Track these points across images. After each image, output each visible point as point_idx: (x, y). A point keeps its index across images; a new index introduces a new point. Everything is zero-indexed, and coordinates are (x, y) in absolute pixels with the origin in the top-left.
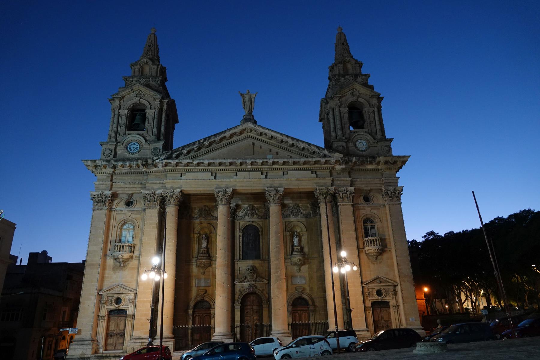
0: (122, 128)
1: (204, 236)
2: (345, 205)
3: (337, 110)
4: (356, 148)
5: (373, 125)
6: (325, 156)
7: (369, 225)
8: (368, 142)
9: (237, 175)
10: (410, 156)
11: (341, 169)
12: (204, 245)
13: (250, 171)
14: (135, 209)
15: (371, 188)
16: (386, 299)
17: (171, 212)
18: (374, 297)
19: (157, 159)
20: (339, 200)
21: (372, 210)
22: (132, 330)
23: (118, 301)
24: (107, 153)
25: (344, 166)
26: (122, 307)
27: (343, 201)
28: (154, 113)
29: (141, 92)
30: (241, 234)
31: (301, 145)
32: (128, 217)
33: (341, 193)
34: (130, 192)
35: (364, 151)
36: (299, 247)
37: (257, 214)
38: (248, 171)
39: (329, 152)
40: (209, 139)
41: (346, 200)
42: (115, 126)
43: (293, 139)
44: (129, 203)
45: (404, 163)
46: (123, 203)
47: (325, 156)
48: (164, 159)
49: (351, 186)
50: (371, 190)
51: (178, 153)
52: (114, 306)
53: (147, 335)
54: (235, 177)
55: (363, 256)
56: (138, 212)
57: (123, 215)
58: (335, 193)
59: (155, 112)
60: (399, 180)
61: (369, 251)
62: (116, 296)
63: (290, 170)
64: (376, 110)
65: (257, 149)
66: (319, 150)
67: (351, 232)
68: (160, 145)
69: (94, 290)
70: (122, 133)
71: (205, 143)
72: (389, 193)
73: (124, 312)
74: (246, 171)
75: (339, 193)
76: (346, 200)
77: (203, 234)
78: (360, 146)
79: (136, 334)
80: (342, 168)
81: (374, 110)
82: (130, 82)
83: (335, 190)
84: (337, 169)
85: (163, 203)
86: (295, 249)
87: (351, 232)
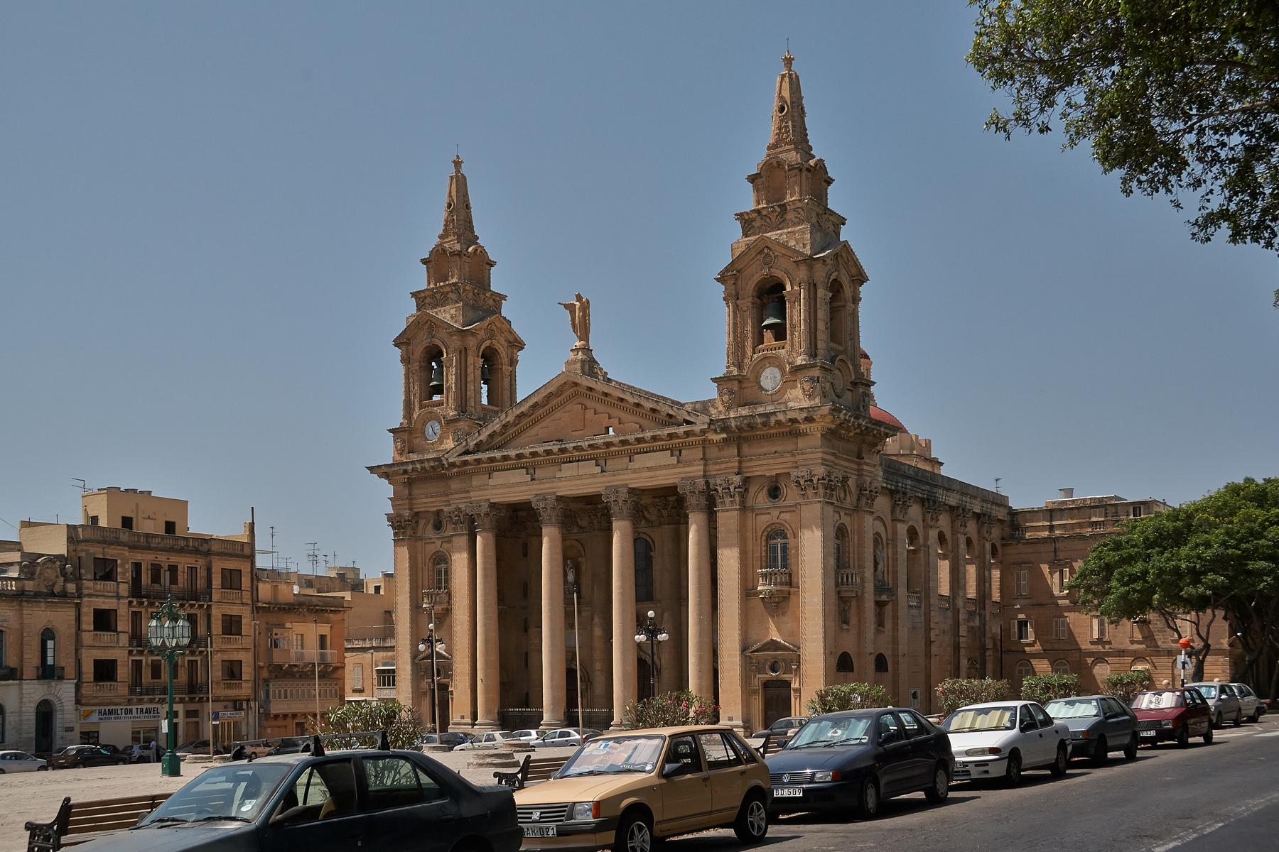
2: (727, 510)
11: (722, 440)
15: (778, 471)
21: (782, 515)
31: (649, 405)
33: (720, 489)
37: (647, 520)
41: (727, 500)
46: (430, 526)
75: (716, 490)
76: (727, 500)
80: (723, 438)
82: (423, 302)
84: (715, 441)
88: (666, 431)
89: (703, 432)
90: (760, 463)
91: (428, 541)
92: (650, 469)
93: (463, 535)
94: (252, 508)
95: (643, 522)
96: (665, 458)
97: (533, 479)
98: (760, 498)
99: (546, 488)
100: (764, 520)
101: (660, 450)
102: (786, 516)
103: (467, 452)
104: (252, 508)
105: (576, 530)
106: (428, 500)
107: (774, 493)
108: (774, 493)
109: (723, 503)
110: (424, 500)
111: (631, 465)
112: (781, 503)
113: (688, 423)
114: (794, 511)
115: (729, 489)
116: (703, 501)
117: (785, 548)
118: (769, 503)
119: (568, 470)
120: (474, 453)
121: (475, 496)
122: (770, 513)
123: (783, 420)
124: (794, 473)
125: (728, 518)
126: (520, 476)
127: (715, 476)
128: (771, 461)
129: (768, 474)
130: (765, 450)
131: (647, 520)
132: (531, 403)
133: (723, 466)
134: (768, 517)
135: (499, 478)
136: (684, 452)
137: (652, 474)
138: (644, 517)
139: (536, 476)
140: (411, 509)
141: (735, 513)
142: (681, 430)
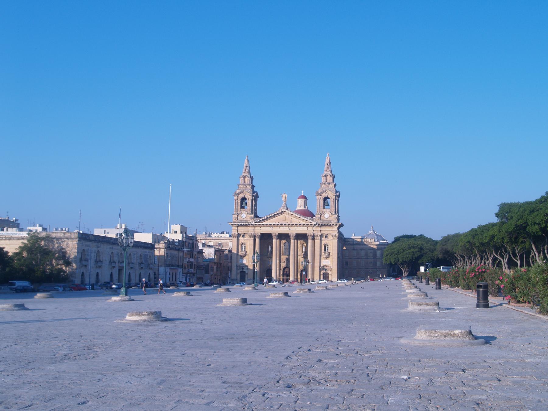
0: (239, 208)
3: (319, 200)
4: (325, 217)
5: (332, 207)
8: (329, 215)
17: (257, 241)
20: (315, 238)
22: (248, 277)
23: (243, 269)
24: (235, 218)
26: (244, 270)
27: (317, 238)
34: (244, 233)
42: (236, 207)
44: (243, 236)
50: (328, 234)
52: (241, 270)
53: (252, 279)
55: (322, 257)
62: (242, 267)
65: (287, 218)
68: (253, 216)
69: (235, 265)
70: (239, 210)
73: (245, 272)
76: (318, 238)
79: (249, 278)
103: (257, 222)
108: (326, 237)
117: (328, 248)
119: (281, 228)
120: (258, 222)
130: (325, 229)
140: (237, 232)
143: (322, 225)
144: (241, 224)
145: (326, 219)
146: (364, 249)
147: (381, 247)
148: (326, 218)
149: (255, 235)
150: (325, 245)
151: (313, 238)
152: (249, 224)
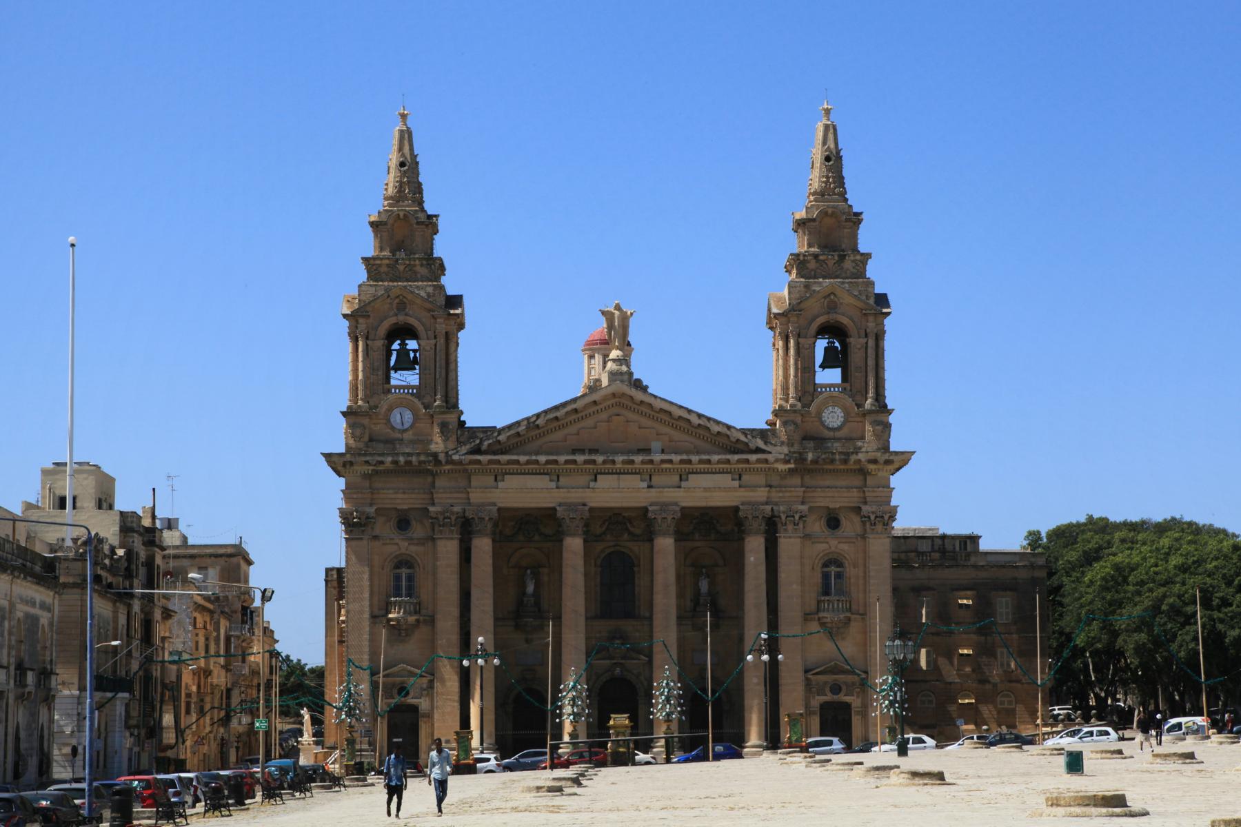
1: (529, 572)
2: (790, 537)
4: (822, 423)
6: (758, 450)
7: (833, 570)
9: (596, 480)
10: (914, 452)
12: (530, 588)
13: (620, 473)
14: (415, 536)
16: (848, 699)
17: (483, 546)
18: (826, 695)
19: (454, 454)
20: (779, 525)
25: (792, 466)
28: (433, 347)
29: (405, 300)
30: (599, 569)
32: (403, 551)
33: (783, 517)
34: (405, 507)
35: (839, 429)
36: (710, 598)
37: (630, 533)
38: (616, 473)
39: (766, 443)
40: (545, 416)
41: (790, 527)
43: (700, 416)
45: (906, 462)
47: (758, 450)
48: (466, 454)
49: (803, 503)
51: (491, 441)
54: (592, 484)
56: (422, 542)
57: (395, 547)
58: (773, 516)
59: (436, 345)
60: (894, 493)
61: (825, 620)
63: (693, 473)
64: (871, 343)
66: (746, 437)
67: (794, 586)
71: (537, 423)
72: (872, 517)
74: (612, 473)
75: (780, 517)
76: (790, 527)
77: (527, 568)
78: (831, 419)
81: (867, 343)
83: (772, 509)
85: (466, 529)
86: (701, 601)
87: (794, 586)
88: (737, 457)
89: (777, 461)
90: (822, 495)
91: (388, 541)
92: (706, 489)
93: (452, 539)
94: (154, 489)
95: (626, 536)
96: (725, 480)
97: (557, 488)
98: (817, 526)
99: (575, 496)
100: (821, 547)
101: (720, 473)
102: (845, 547)
104: (154, 489)
105: (537, 538)
106: (400, 496)
107: (833, 522)
108: (833, 522)
109: (786, 530)
110: (393, 496)
111: (684, 484)
112: (839, 532)
113: (763, 451)
114: (854, 543)
115: (793, 517)
116: (763, 527)
118: (827, 533)
121: (476, 497)
122: (828, 543)
123: (863, 460)
124: (866, 509)
125: (788, 545)
126: (542, 482)
127: (776, 504)
128: (836, 495)
129: (831, 506)
130: (828, 483)
131: (630, 533)
132: (569, 408)
133: (787, 494)
134: (824, 546)
135: (511, 482)
136: (744, 477)
137: (708, 494)
138: (627, 529)
139: (560, 483)
141: (799, 540)
142: (753, 457)
143: (815, 462)
144: (395, 462)
145: (831, 434)
146: (928, 589)
147: (1015, 579)
148: (829, 429)
149: (469, 515)
150: (825, 565)
151: (772, 528)
152: (437, 462)
